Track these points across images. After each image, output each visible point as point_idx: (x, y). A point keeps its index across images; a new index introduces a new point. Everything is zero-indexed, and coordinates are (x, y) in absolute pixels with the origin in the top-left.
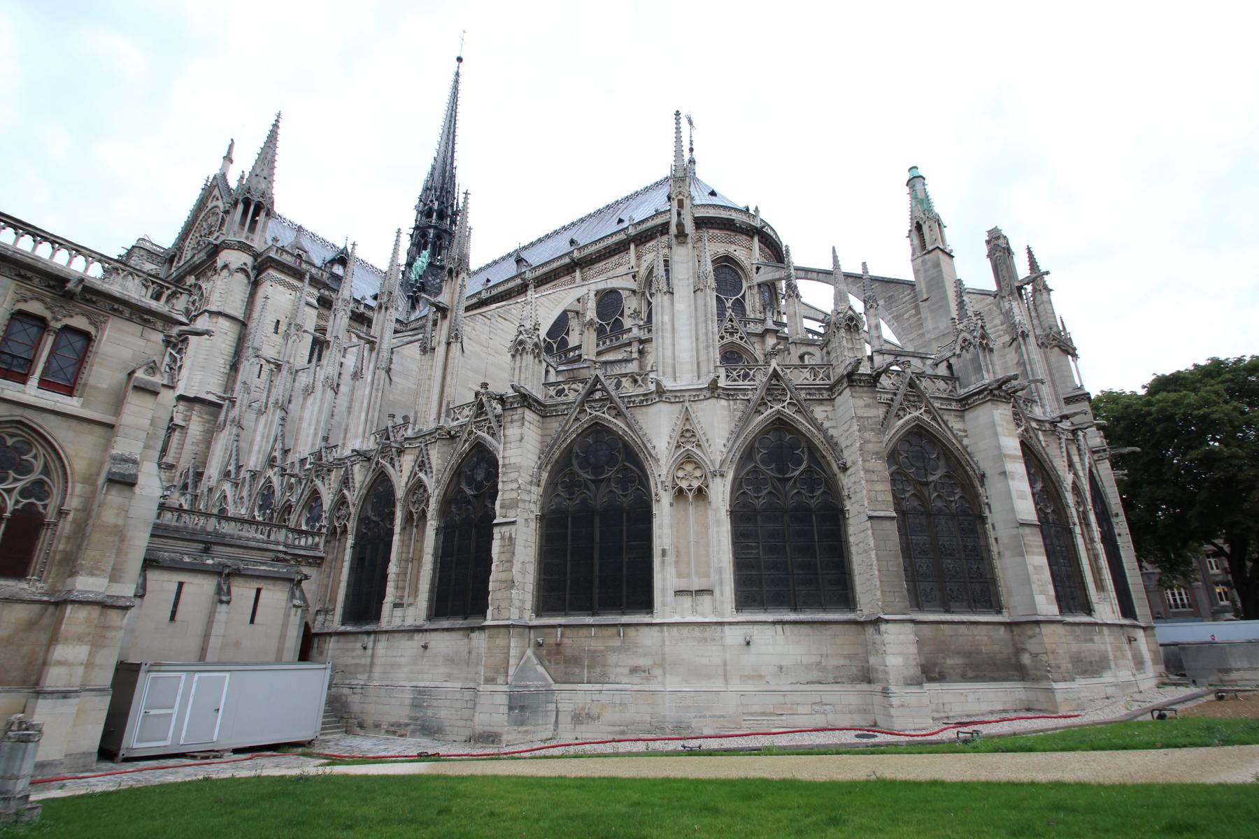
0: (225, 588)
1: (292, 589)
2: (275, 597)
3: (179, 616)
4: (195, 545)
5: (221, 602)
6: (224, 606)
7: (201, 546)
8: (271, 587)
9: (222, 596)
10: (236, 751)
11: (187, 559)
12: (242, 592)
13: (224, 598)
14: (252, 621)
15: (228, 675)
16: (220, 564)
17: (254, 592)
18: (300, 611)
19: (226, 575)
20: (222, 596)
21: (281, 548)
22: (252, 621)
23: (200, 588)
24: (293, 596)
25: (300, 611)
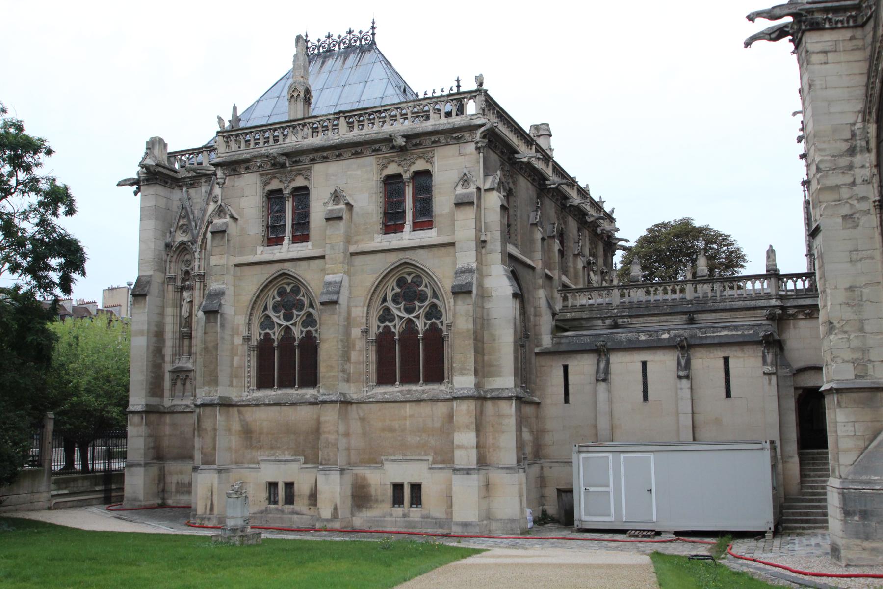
0: (683, 362)
1: (764, 353)
2: (748, 366)
3: (649, 398)
4: (679, 317)
5: (680, 377)
6: (684, 381)
7: (685, 317)
8: (740, 354)
9: (685, 372)
10: (678, 534)
11: (643, 337)
12: (707, 364)
13: (682, 373)
14: (728, 394)
15: (652, 455)
16: (675, 336)
17: (721, 363)
18: (774, 378)
19: (684, 347)
20: (685, 372)
21: (773, 302)
22: (728, 394)
23: (663, 364)
24: (765, 362)
25: (774, 378)
